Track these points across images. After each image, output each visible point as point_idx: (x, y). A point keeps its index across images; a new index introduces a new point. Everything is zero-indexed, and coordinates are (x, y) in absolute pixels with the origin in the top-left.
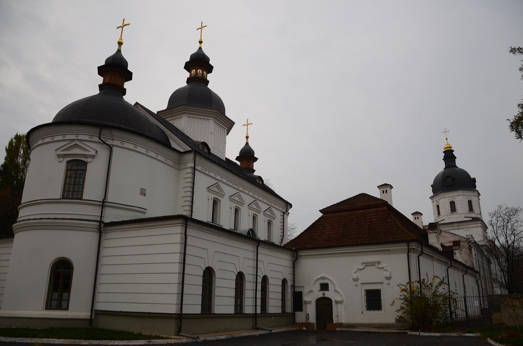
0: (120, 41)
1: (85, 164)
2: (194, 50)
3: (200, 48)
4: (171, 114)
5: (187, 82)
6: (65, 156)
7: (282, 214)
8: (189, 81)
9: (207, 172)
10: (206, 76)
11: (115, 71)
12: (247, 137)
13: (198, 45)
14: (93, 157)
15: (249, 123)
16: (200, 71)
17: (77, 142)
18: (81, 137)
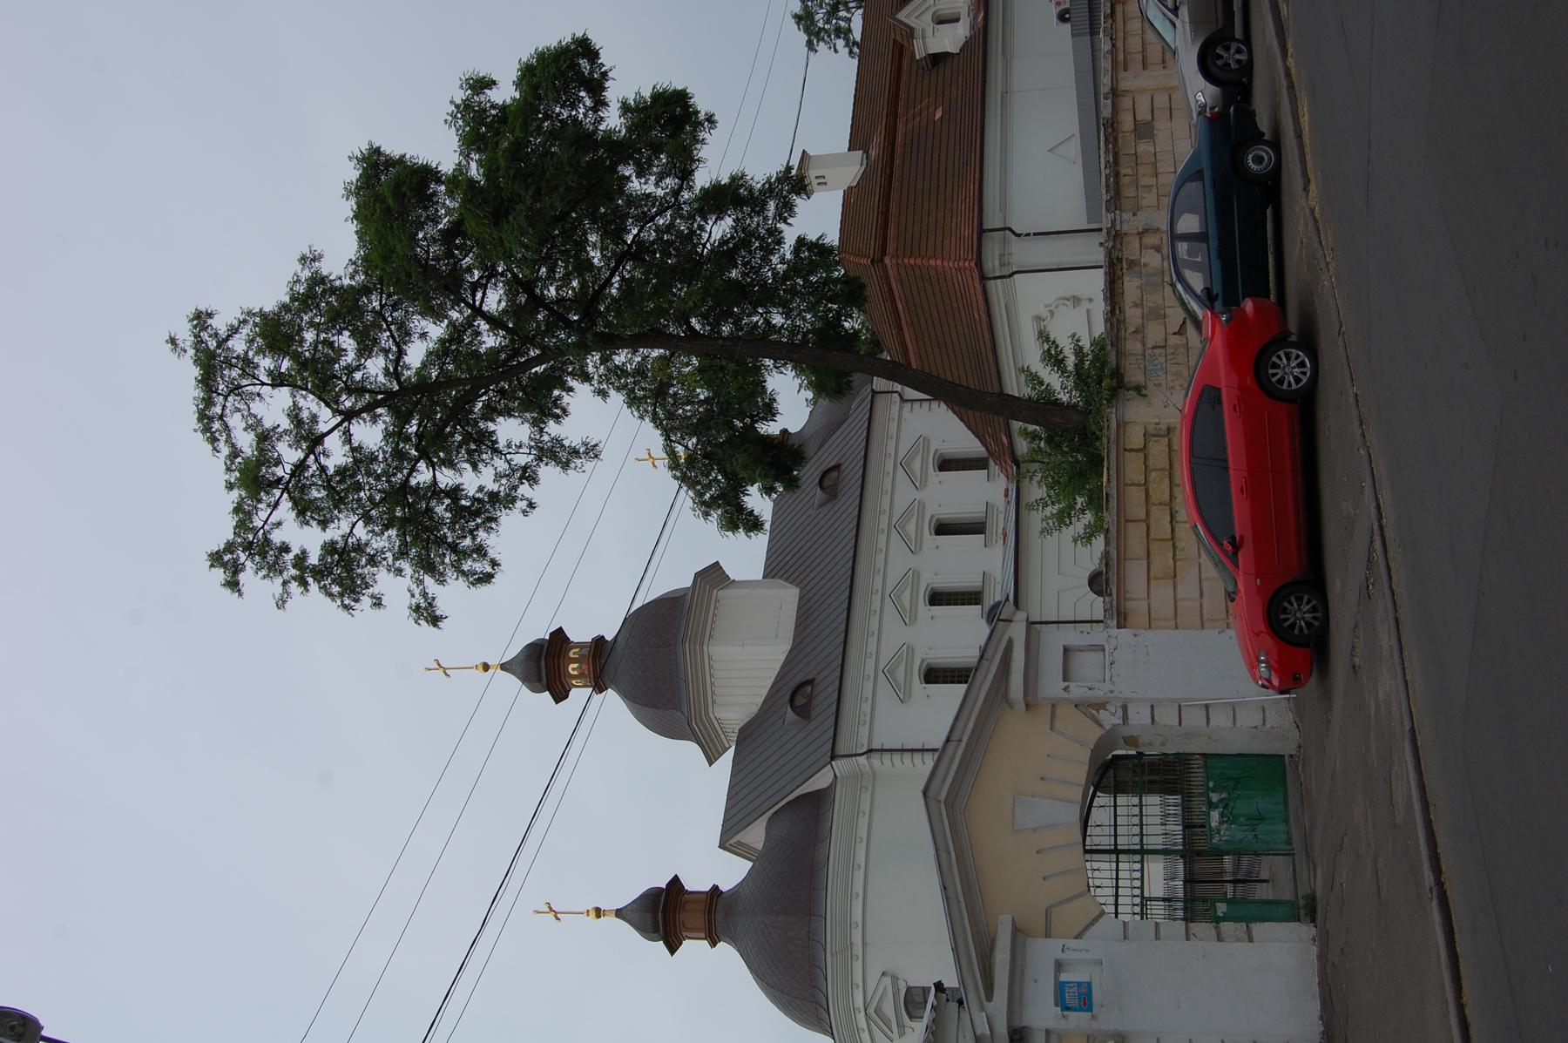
0: (593, 914)
1: (909, 989)
2: (512, 682)
3: (504, 667)
6: (901, 1026)
7: (907, 406)
9: (867, 707)
10: (580, 645)
11: (667, 914)
14: (895, 978)
16: (572, 668)
17: (871, 1011)
18: (859, 1003)
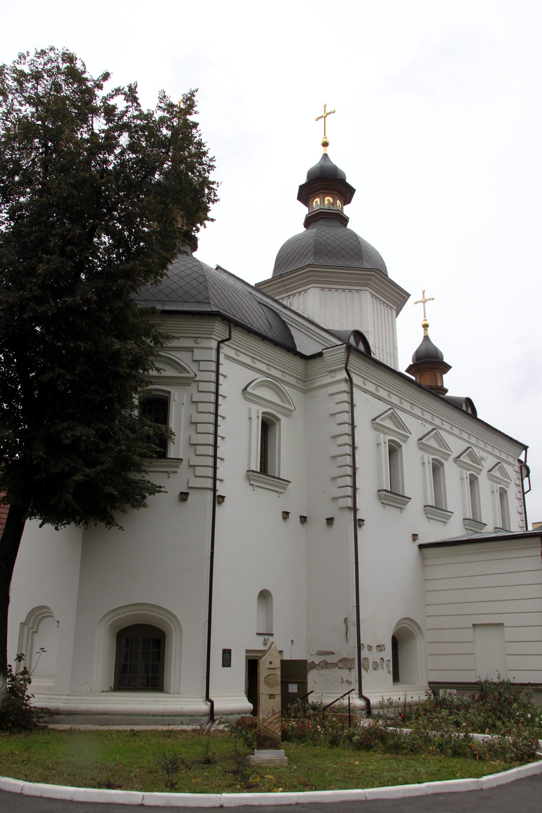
3: (325, 156)
4: (284, 285)
5: (305, 227)
8: (309, 222)
10: (342, 208)
12: (426, 326)
13: (322, 151)
15: (427, 297)
16: (328, 199)
